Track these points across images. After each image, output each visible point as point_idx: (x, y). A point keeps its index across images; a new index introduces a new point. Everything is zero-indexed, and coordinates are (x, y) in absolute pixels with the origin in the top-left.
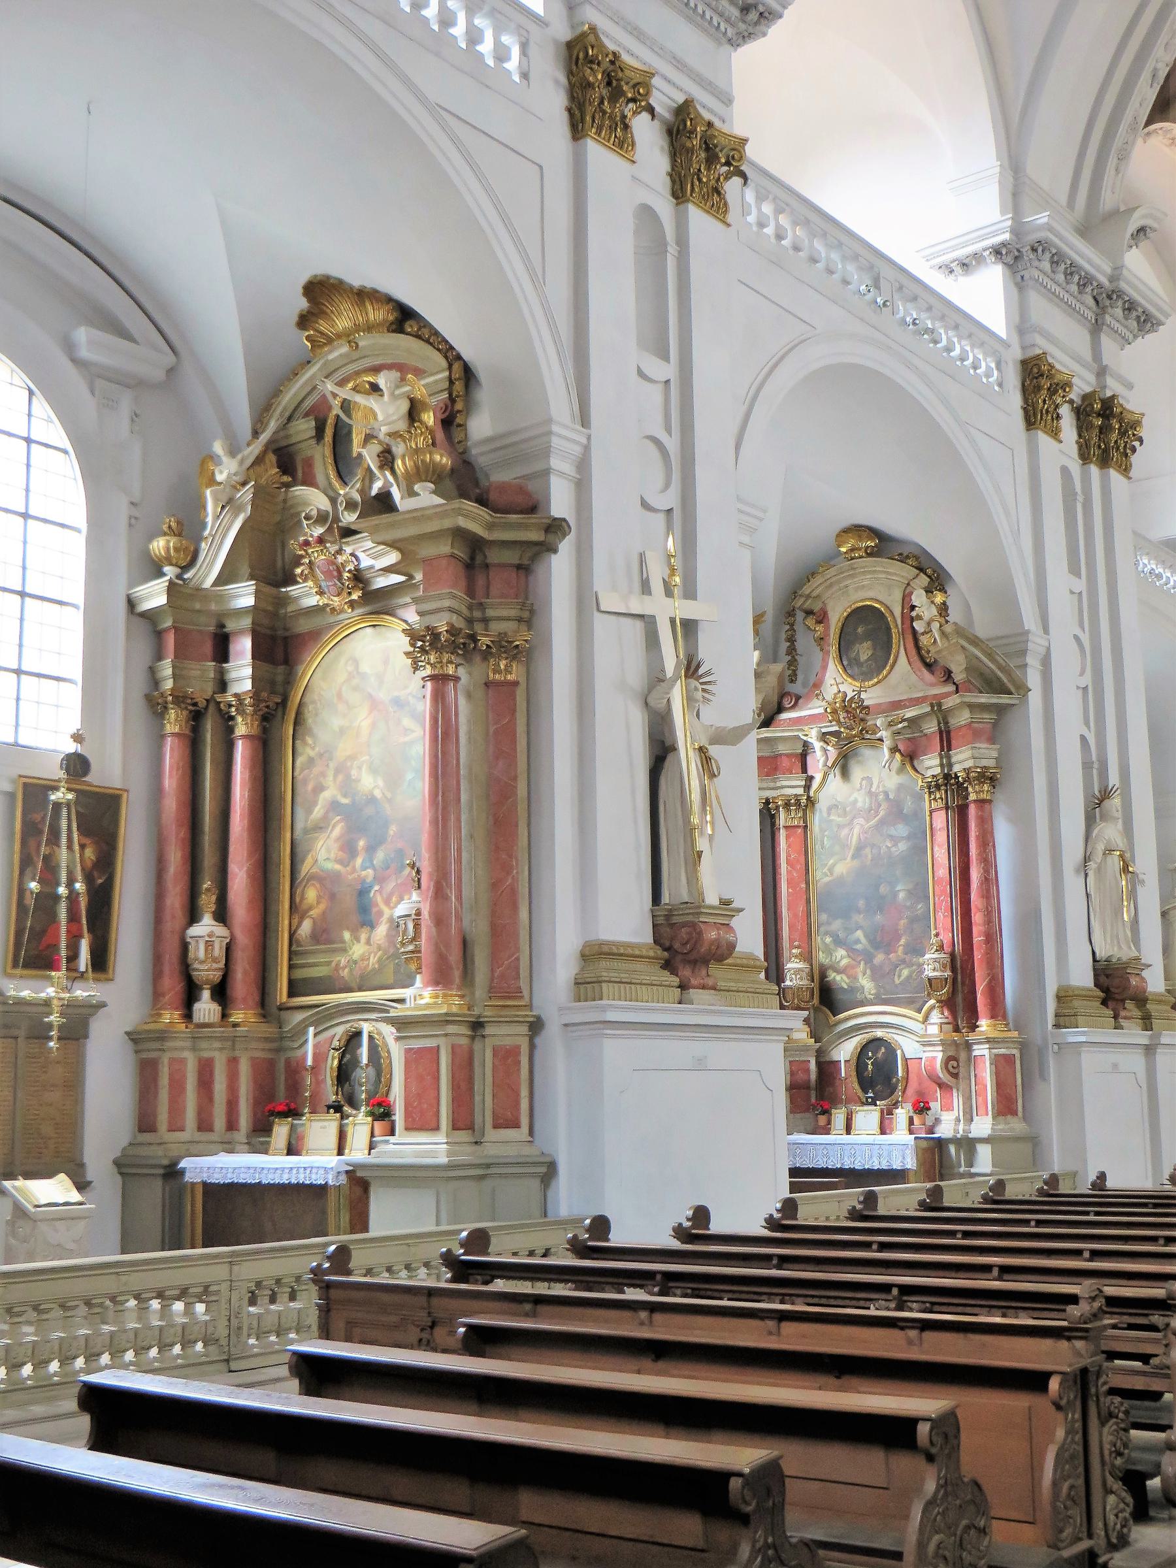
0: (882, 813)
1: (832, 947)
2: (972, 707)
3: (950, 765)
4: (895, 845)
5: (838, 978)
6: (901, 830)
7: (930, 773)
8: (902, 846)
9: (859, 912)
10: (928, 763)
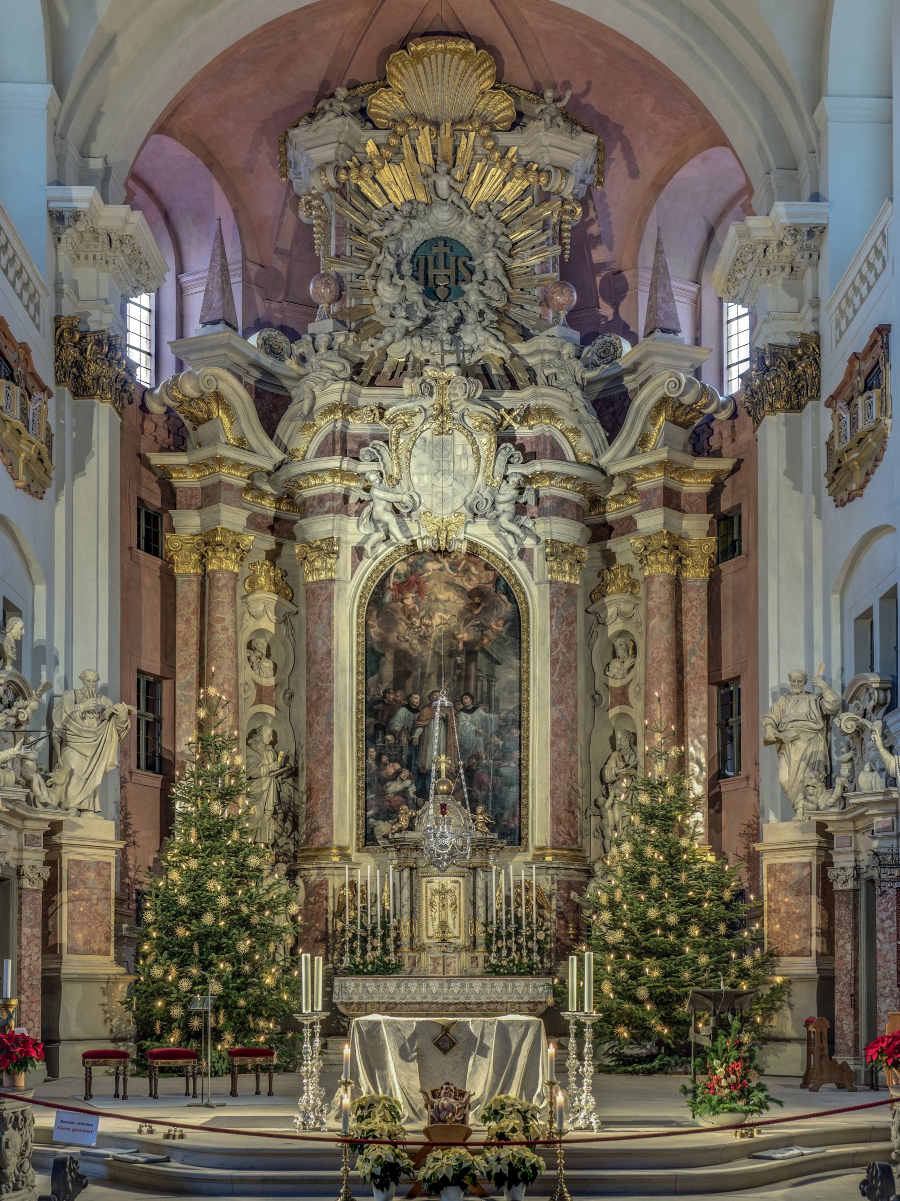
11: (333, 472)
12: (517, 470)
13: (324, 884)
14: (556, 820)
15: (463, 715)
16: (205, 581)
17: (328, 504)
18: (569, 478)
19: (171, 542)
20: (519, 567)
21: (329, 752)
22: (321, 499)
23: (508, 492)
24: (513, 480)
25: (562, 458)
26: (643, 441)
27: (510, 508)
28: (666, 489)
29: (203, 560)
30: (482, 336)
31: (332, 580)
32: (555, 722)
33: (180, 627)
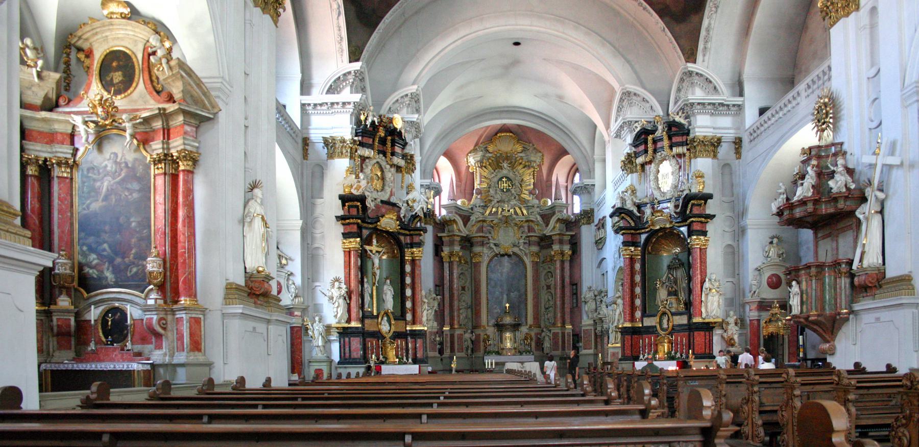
0: (123, 174)
1: (87, 253)
2: (185, 113)
3: (169, 149)
4: (131, 194)
5: (91, 271)
6: (135, 186)
7: (156, 152)
8: (135, 195)
9: (106, 233)
10: (154, 147)
11: (480, 236)
12: (524, 236)
13: (480, 334)
14: (534, 318)
15: (512, 294)
16: (451, 263)
17: (479, 244)
18: (536, 236)
19: (443, 254)
20: (525, 258)
21: (480, 303)
22: (477, 242)
23: (522, 241)
24: (523, 237)
25: (535, 232)
26: (554, 227)
27: (523, 244)
28: (560, 239)
29: (450, 257)
30: (515, 202)
31: (480, 262)
32: (534, 295)
33: (445, 274)
